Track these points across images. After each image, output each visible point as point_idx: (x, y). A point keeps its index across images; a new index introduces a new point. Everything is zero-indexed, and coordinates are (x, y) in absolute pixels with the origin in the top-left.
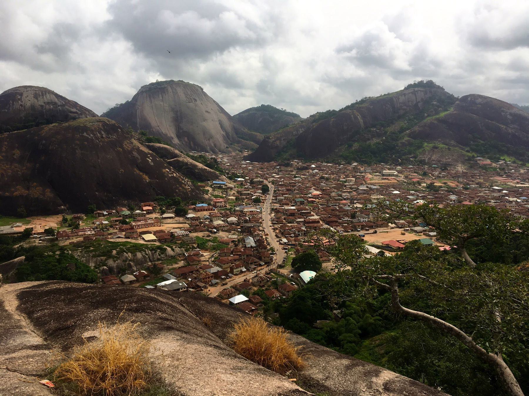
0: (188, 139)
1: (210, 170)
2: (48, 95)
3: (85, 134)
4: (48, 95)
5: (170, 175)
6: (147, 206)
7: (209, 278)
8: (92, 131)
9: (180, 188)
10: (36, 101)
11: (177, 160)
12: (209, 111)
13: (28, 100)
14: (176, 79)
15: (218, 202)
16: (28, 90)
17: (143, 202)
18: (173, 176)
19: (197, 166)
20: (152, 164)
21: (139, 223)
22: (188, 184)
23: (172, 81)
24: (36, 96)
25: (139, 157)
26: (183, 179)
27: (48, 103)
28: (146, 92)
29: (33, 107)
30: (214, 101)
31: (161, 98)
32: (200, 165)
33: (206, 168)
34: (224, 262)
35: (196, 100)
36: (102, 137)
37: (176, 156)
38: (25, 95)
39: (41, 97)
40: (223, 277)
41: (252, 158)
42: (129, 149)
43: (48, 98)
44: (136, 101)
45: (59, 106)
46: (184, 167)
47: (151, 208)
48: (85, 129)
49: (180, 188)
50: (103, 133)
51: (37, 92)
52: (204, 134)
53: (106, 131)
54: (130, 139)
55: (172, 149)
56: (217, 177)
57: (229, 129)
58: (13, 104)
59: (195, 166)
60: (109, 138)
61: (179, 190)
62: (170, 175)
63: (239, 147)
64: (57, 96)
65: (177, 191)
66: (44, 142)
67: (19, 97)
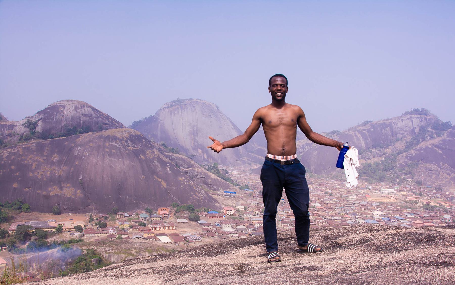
1: (222, 180)
2: (86, 108)
3: (114, 143)
4: (86, 108)
5: (186, 183)
8: (121, 141)
9: (194, 196)
10: (76, 112)
11: (192, 170)
13: (69, 112)
16: (70, 103)
17: (161, 206)
18: (188, 184)
19: (210, 176)
20: (170, 172)
21: (156, 226)
24: (76, 109)
25: (159, 166)
26: (196, 187)
27: (85, 115)
29: (73, 118)
30: (228, 118)
31: (181, 114)
32: (213, 176)
33: (218, 178)
36: (129, 146)
37: (191, 166)
39: (80, 110)
42: (151, 158)
43: (86, 110)
44: (159, 116)
45: (94, 118)
47: (167, 212)
48: (115, 138)
49: (194, 196)
50: (129, 142)
51: (78, 105)
53: (131, 140)
54: (153, 149)
55: (188, 159)
58: (57, 115)
59: (208, 176)
60: (135, 147)
61: (193, 197)
62: (186, 183)
63: (248, 160)
64: (93, 109)
65: (191, 198)
66: (79, 148)
67: (62, 109)
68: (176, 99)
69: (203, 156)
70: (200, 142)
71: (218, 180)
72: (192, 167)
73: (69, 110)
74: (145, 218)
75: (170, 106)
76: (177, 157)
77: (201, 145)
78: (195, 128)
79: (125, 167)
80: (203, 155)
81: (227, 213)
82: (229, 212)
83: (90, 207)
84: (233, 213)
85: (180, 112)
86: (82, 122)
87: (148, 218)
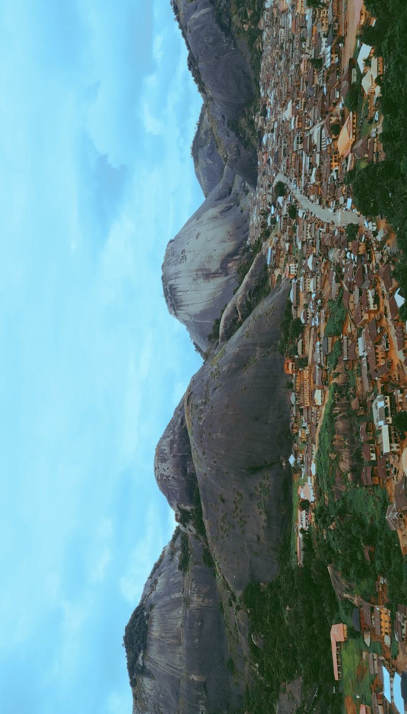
0: (230, 262)
6: (288, 367)
7: (377, 354)
10: (168, 461)
12: (197, 234)
13: (168, 468)
14: (160, 273)
15: (290, 272)
17: (283, 369)
19: (247, 282)
22: (264, 306)
23: (163, 278)
28: (175, 310)
30: (186, 225)
31: (182, 293)
32: (247, 278)
34: (360, 316)
35: (183, 252)
38: (163, 472)
40: (379, 331)
41: (254, 183)
45: (174, 437)
46: (249, 300)
52: (224, 242)
56: (264, 257)
57: (222, 206)
68: (164, 299)
69: (237, 260)
70: (218, 266)
71: (252, 270)
72: (236, 307)
73: (166, 469)
74: (296, 399)
75: (172, 307)
76: (225, 327)
77: (221, 265)
78: (200, 273)
79: (230, 413)
80: (234, 260)
81: (294, 273)
82: (292, 270)
83: (284, 464)
84: (293, 265)
85: (179, 294)
86: (179, 454)
87: (297, 394)
